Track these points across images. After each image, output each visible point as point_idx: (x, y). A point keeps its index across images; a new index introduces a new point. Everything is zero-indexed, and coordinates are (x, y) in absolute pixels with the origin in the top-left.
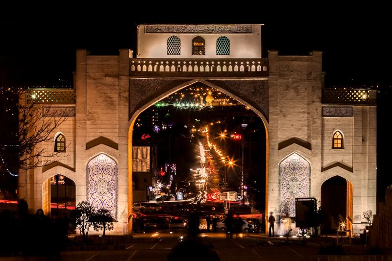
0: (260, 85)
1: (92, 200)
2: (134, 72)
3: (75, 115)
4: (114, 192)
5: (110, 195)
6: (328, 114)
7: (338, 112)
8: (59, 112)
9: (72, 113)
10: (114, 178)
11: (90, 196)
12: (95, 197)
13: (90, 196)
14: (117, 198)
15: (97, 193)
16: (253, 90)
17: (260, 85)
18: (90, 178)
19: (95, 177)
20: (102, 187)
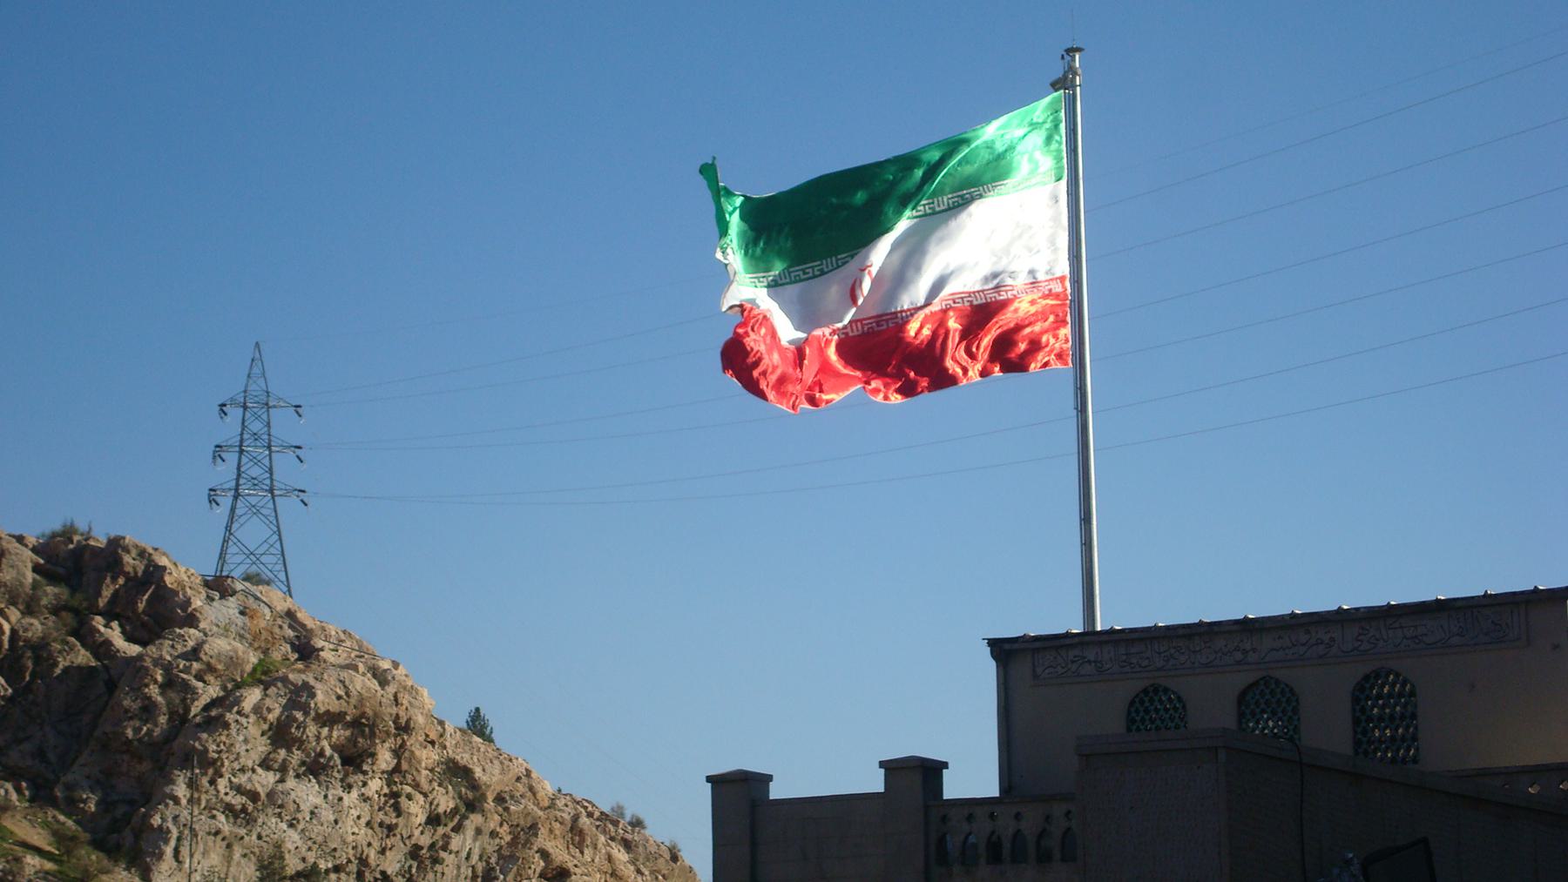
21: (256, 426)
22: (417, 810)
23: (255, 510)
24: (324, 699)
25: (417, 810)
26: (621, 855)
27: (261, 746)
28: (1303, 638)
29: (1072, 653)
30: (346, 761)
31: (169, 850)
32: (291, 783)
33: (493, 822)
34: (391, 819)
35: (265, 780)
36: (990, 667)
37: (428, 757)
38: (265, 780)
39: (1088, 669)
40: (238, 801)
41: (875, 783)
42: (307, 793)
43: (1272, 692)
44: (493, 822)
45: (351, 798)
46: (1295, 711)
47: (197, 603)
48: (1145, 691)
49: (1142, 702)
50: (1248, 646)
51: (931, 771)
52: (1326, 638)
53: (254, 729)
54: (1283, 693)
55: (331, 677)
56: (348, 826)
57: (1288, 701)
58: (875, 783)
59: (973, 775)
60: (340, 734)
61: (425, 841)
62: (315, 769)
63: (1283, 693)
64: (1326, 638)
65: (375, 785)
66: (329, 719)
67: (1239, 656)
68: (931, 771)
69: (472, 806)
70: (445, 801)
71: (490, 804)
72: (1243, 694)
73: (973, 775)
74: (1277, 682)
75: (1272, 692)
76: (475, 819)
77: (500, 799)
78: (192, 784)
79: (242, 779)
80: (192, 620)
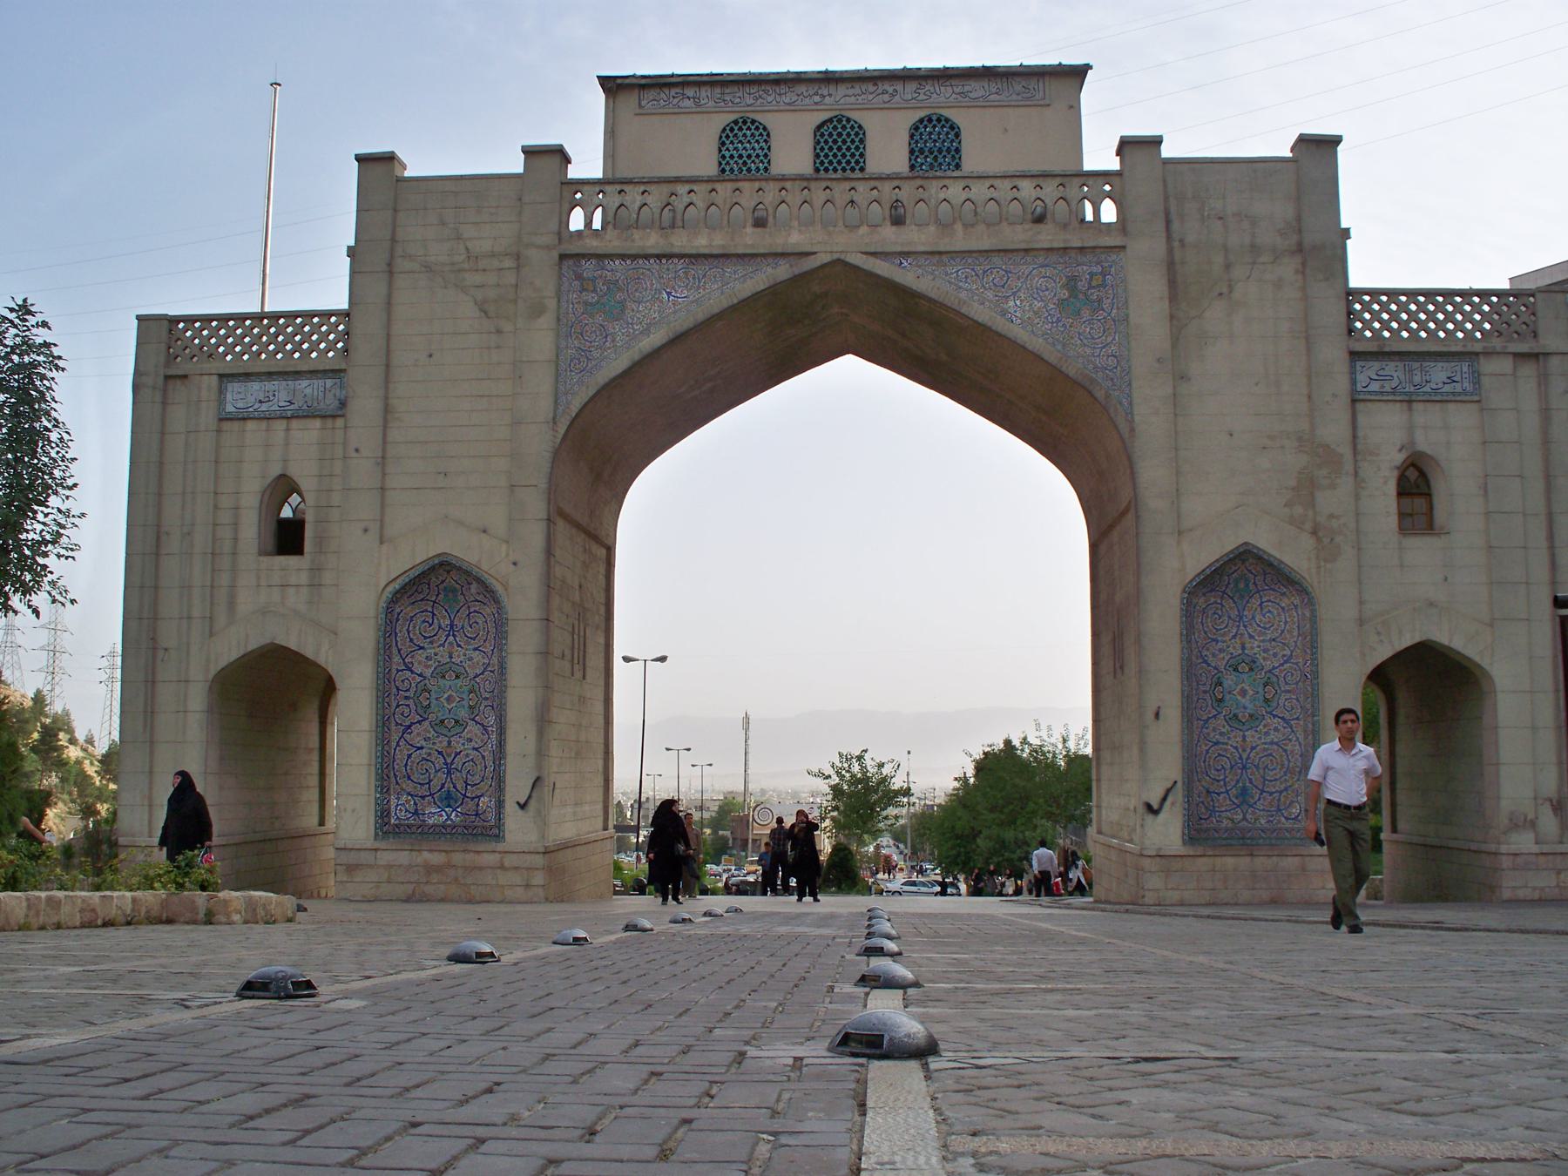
0: (1092, 275)
1: (404, 750)
2: (579, 232)
3: (343, 404)
4: (492, 720)
5: (477, 729)
6: (1375, 387)
7: (1417, 379)
8: (283, 397)
9: (330, 403)
10: (495, 660)
11: (395, 737)
12: (420, 742)
13: (395, 737)
14: (501, 744)
15: (426, 723)
16: (1065, 294)
17: (1092, 275)
18: (396, 659)
19: (420, 656)
20: (449, 699)
28: (871, 88)
29: (673, 91)
36: (600, 96)
39: (687, 103)
41: (516, 165)
43: (844, 128)
46: (862, 141)
48: (736, 122)
49: (732, 130)
50: (825, 92)
52: (890, 90)
54: (852, 128)
57: (857, 134)
58: (516, 165)
63: (852, 128)
64: (890, 90)
67: (817, 98)
68: (559, 155)
72: (819, 127)
74: (848, 120)
75: (844, 128)
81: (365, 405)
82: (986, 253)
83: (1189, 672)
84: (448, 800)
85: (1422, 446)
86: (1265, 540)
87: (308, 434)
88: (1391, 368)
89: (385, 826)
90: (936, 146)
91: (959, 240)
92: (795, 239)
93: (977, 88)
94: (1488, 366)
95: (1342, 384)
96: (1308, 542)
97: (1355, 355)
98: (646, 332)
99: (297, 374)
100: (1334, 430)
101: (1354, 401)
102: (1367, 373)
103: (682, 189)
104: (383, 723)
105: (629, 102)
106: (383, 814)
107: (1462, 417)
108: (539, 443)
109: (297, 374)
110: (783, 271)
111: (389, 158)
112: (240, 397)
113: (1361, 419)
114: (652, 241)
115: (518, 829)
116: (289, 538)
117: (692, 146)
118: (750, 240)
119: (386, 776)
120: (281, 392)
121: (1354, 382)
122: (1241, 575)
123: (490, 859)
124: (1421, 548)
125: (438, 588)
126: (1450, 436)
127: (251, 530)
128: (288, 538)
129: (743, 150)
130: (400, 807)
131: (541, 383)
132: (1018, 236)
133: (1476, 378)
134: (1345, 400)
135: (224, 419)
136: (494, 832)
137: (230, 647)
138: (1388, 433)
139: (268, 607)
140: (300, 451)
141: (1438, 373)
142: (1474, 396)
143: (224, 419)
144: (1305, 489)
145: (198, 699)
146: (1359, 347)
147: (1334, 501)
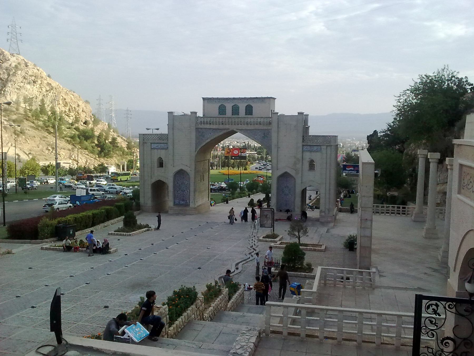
21: (14, 30)
22: (44, 90)
23: (14, 42)
24: (30, 73)
25: (44, 90)
26: (72, 96)
27: (21, 80)
30: (34, 82)
31: (9, 94)
32: (26, 85)
33: (55, 92)
34: (41, 90)
35: (22, 84)
37: (45, 82)
38: (22, 84)
40: (18, 87)
42: (28, 86)
44: (55, 92)
45: (35, 87)
47: (10, 57)
51: (196, 113)
53: (20, 77)
55: (31, 70)
56: (34, 91)
59: (200, 114)
60: (33, 78)
61: (45, 94)
62: (29, 83)
65: (38, 86)
66: (31, 76)
68: (196, 113)
69: (52, 89)
70: (48, 89)
71: (54, 89)
73: (200, 114)
76: (52, 91)
77: (56, 89)
78: (12, 85)
79: (19, 84)
80: (9, 60)
81: (170, 147)
82: (253, 130)
83: (278, 188)
84: (183, 200)
85: (312, 158)
86: (289, 171)
87: (163, 151)
88: (308, 147)
89: (175, 204)
90: (249, 110)
91: (250, 127)
92: (227, 126)
93: (255, 100)
94: (322, 147)
95: (301, 149)
96: (294, 171)
97: (303, 145)
98: (207, 139)
99: (161, 143)
100: (299, 156)
101: (303, 152)
102: (305, 147)
103: (212, 119)
104: (174, 191)
105: (206, 101)
106: (175, 202)
107: (318, 154)
108: (194, 154)
109: (161, 143)
110: (225, 131)
111: (172, 113)
112: (154, 146)
113: (304, 154)
114: (208, 126)
115: (192, 205)
116: (161, 164)
117: (214, 110)
118: (221, 127)
119: (175, 197)
120: (160, 145)
121: (303, 149)
122: (285, 176)
123: (188, 209)
124: (311, 173)
125: (181, 174)
126: (316, 157)
127: (156, 164)
128: (161, 164)
129: (222, 110)
130: (177, 201)
131: (194, 145)
132: (257, 127)
133: (321, 149)
134: (301, 152)
135: (152, 149)
136: (189, 205)
137: (154, 180)
138: (308, 156)
139: (159, 175)
140: (162, 154)
141: (315, 148)
142: (320, 151)
143: (152, 149)
144: (295, 164)
145: (150, 187)
146: (303, 144)
147: (299, 166)
